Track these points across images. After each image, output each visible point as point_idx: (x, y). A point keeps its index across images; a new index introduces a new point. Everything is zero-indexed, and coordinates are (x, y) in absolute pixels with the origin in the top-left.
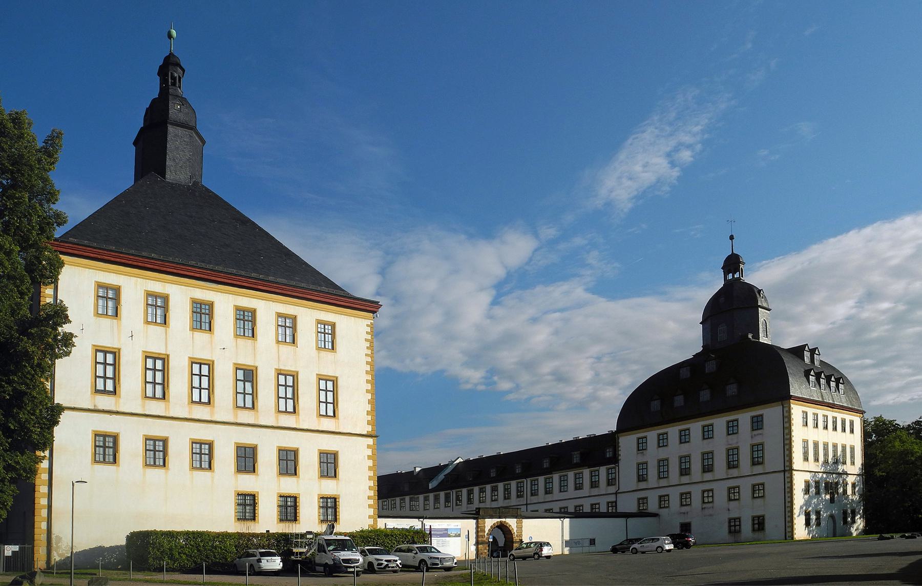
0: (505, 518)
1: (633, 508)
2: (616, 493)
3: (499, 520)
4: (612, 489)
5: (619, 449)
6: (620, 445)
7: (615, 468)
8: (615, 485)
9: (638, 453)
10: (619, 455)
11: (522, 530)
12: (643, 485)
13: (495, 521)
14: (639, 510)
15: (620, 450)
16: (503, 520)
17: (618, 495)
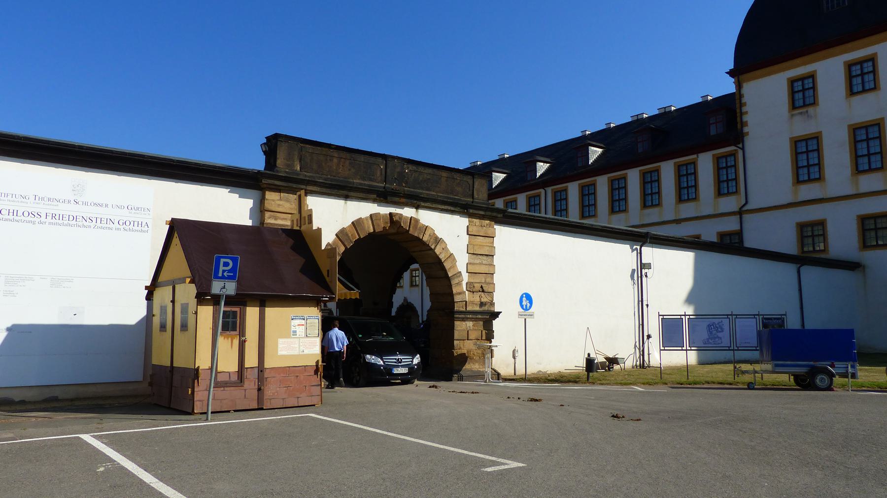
0: (417, 202)
1: (788, 244)
2: (740, 213)
3: (385, 210)
4: (730, 204)
5: (744, 109)
6: (743, 101)
7: (733, 154)
8: (736, 192)
9: (792, 115)
10: (744, 124)
11: (492, 265)
12: (808, 191)
13: (363, 210)
14: (803, 252)
15: (746, 113)
16: (408, 212)
17: (746, 217)
